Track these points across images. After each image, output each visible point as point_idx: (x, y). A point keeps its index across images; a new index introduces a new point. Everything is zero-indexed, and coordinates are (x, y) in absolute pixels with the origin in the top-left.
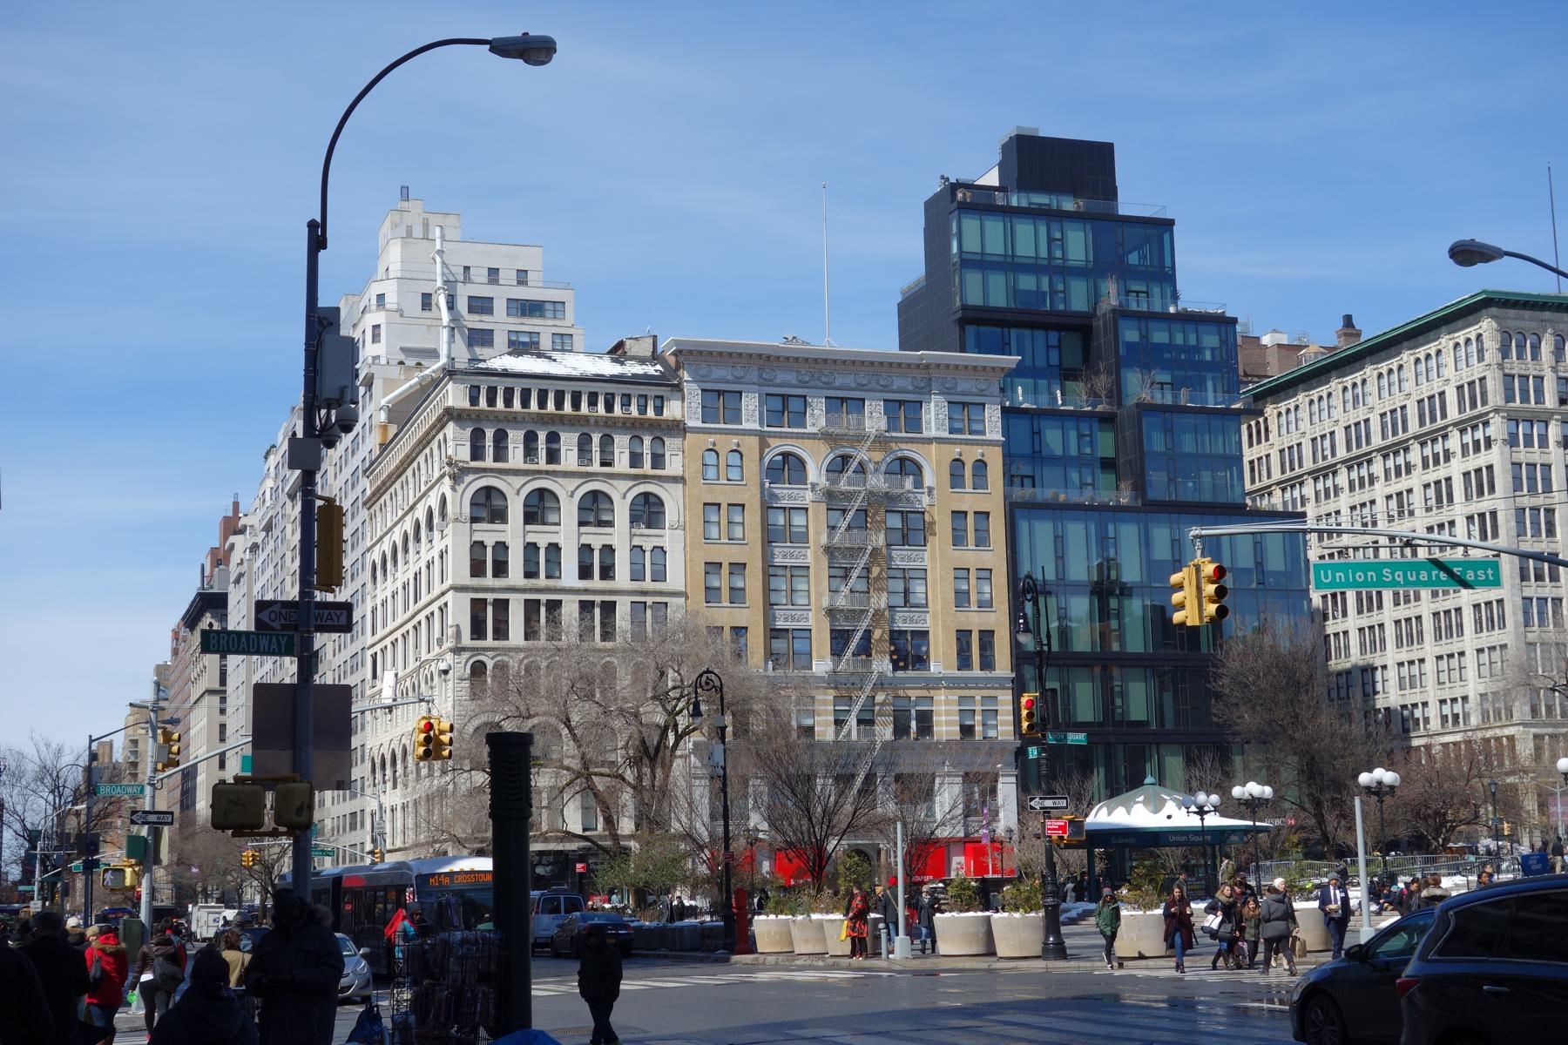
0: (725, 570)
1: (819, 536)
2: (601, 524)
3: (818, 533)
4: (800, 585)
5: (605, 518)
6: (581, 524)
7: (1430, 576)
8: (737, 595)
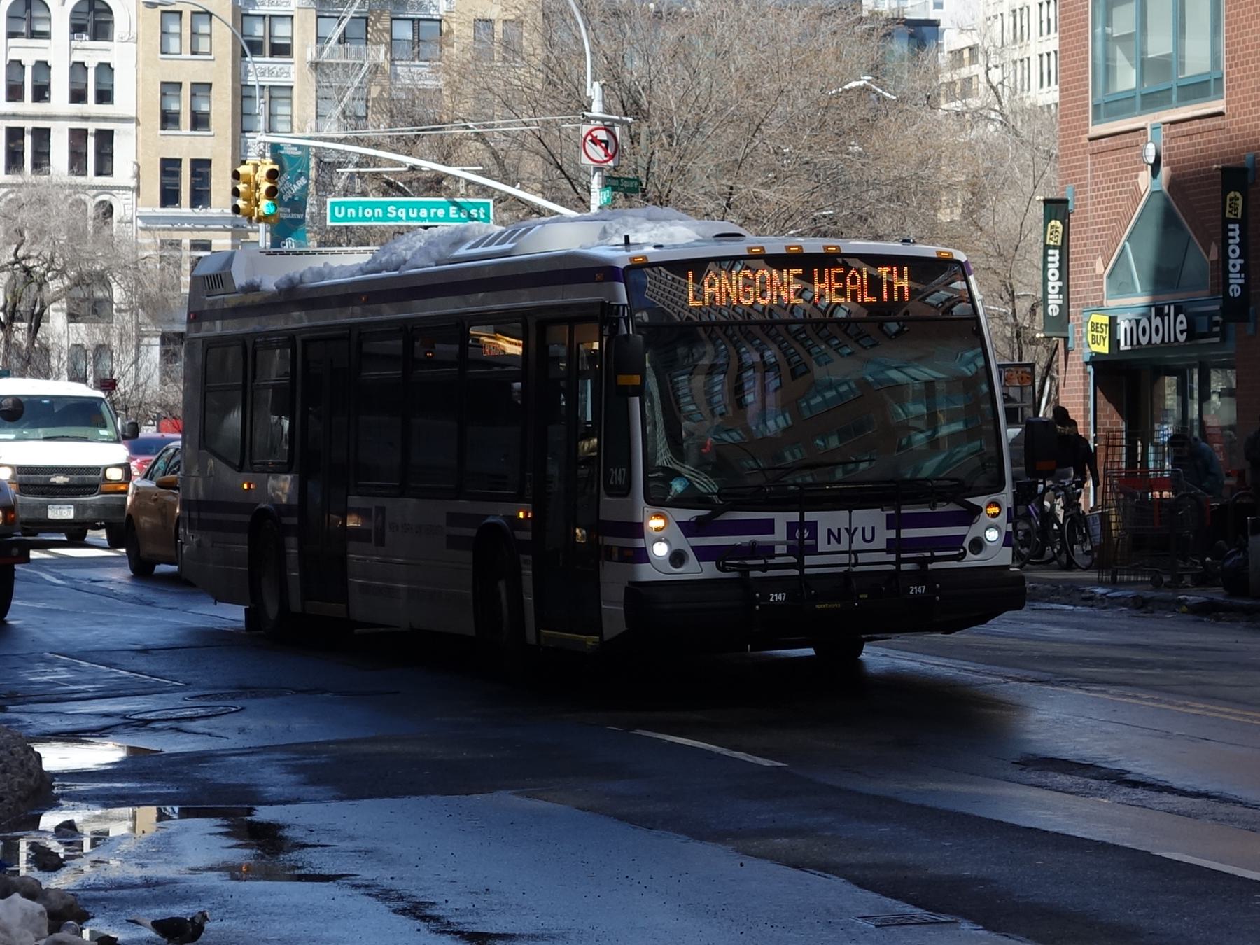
0: (186, 92)
1: (305, 50)
2: (34, 35)
3: (304, 46)
4: (282, 110)
5: (40, 27)
6: (11, 35)
7: (429, 213)
8: (200, 121)
